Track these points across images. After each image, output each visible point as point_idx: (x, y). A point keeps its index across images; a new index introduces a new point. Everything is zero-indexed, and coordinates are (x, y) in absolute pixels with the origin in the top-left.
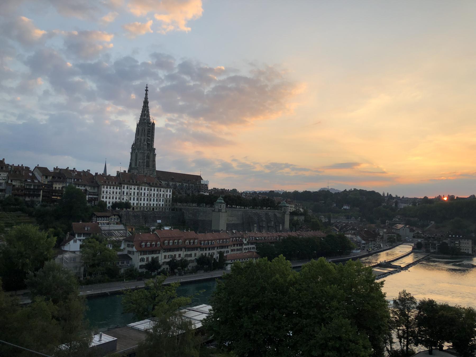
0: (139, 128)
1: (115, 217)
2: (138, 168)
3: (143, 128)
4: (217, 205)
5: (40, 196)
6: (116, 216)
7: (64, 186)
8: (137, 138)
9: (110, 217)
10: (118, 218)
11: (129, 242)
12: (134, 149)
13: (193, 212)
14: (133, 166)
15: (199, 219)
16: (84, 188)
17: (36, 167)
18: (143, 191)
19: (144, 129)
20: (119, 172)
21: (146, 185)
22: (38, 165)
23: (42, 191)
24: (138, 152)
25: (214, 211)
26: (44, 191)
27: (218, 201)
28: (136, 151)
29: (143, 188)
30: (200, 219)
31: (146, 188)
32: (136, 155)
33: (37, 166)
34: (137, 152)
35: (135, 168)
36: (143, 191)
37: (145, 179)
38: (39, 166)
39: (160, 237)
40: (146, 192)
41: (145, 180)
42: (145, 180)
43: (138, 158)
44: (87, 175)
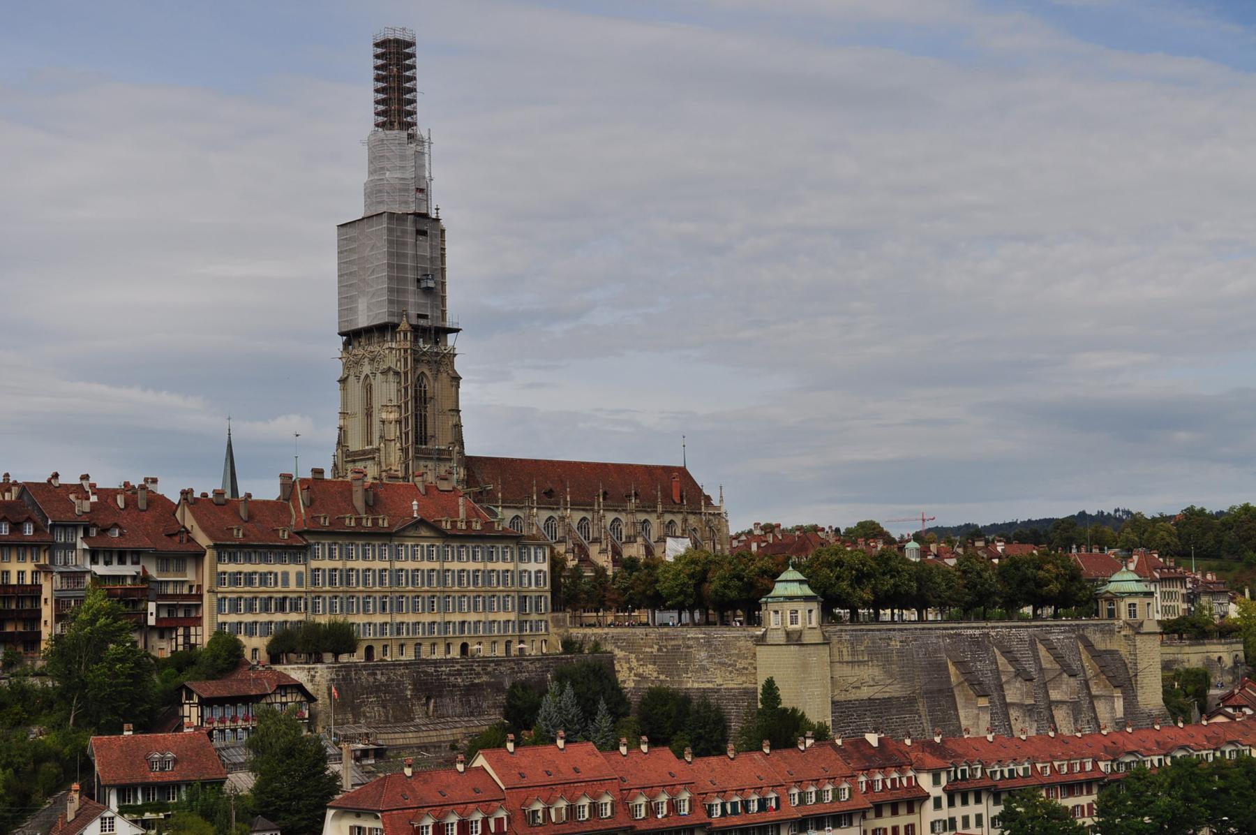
1: (284, 700)
2: (379, 449)
4: (776, 612)
6: (289, 695)
7: (42, 562)
9: (264, 701)
10: (301, 702)
11: (358, 816)
13: (658, 650)
15: (689, 685)
20: (290, 477)
21: (424, 532)
24: (374, 375)
25: (761, 641)
27: (780, 589)
30: (696, 685)
34: (367, 376)
35: (364, 452)
39: (503, 788)
42: (415, 508)
43: (376, 405)
44: (142, 504)
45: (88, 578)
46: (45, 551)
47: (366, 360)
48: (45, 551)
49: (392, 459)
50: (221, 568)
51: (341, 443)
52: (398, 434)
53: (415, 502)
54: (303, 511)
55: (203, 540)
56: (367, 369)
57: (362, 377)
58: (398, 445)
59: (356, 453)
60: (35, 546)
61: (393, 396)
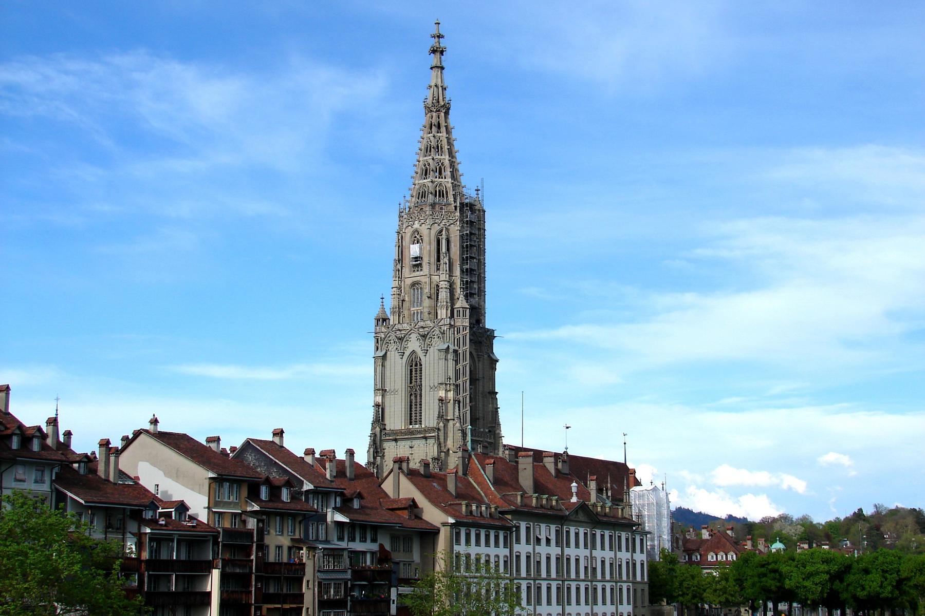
0: (417, 231)
3: (441, 231)
5: (209, 604)
8: (409, 282)
12: (401, 339)
14: (396, 421)
16: (375, 547)
17: (137, 434)
18: (571, 552)
19: (447, 230)
22: (155, 422)
23: (216, 573)
26: (228, 570)
28: (414, 344)
29: (573, 530)
31: (582, 531)
32: (414, 367)
33: (148, 427)
36: (571, 552)
37: (574, 484)
38: (161, 428)
40: (583, 552)
41: (574, 490)
42: (574, 490)
45: (345, 554)
46: (300, 523)
47: (414, 337)
48: (300, 523)
49: (450, 443)
50: (461, 548)
51: (379, 419)
52: (457, 414)
53: (574, 484)
54: (493, 489)
55: (433, 515)
56: (414, 344)
57: (407, 353)
58: (458, 425)
59: (395, 432)
60: (277, 514)
61: (451, 373)
